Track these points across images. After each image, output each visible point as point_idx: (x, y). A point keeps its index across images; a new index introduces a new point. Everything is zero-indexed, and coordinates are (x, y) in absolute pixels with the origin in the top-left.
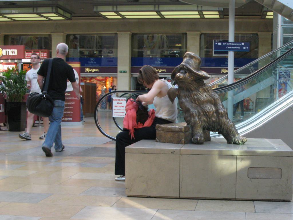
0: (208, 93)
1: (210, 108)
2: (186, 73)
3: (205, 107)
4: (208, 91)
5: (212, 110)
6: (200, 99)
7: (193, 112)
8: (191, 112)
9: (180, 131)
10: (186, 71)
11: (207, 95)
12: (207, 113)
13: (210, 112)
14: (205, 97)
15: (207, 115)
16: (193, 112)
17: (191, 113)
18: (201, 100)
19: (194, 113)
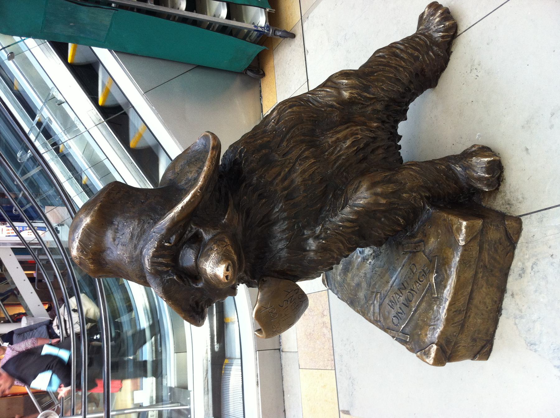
2: (196, 240)
6: (306, 175)
7: (376, 194)
12: (362, 145)
16: (376, 194)
17: (383, 201)
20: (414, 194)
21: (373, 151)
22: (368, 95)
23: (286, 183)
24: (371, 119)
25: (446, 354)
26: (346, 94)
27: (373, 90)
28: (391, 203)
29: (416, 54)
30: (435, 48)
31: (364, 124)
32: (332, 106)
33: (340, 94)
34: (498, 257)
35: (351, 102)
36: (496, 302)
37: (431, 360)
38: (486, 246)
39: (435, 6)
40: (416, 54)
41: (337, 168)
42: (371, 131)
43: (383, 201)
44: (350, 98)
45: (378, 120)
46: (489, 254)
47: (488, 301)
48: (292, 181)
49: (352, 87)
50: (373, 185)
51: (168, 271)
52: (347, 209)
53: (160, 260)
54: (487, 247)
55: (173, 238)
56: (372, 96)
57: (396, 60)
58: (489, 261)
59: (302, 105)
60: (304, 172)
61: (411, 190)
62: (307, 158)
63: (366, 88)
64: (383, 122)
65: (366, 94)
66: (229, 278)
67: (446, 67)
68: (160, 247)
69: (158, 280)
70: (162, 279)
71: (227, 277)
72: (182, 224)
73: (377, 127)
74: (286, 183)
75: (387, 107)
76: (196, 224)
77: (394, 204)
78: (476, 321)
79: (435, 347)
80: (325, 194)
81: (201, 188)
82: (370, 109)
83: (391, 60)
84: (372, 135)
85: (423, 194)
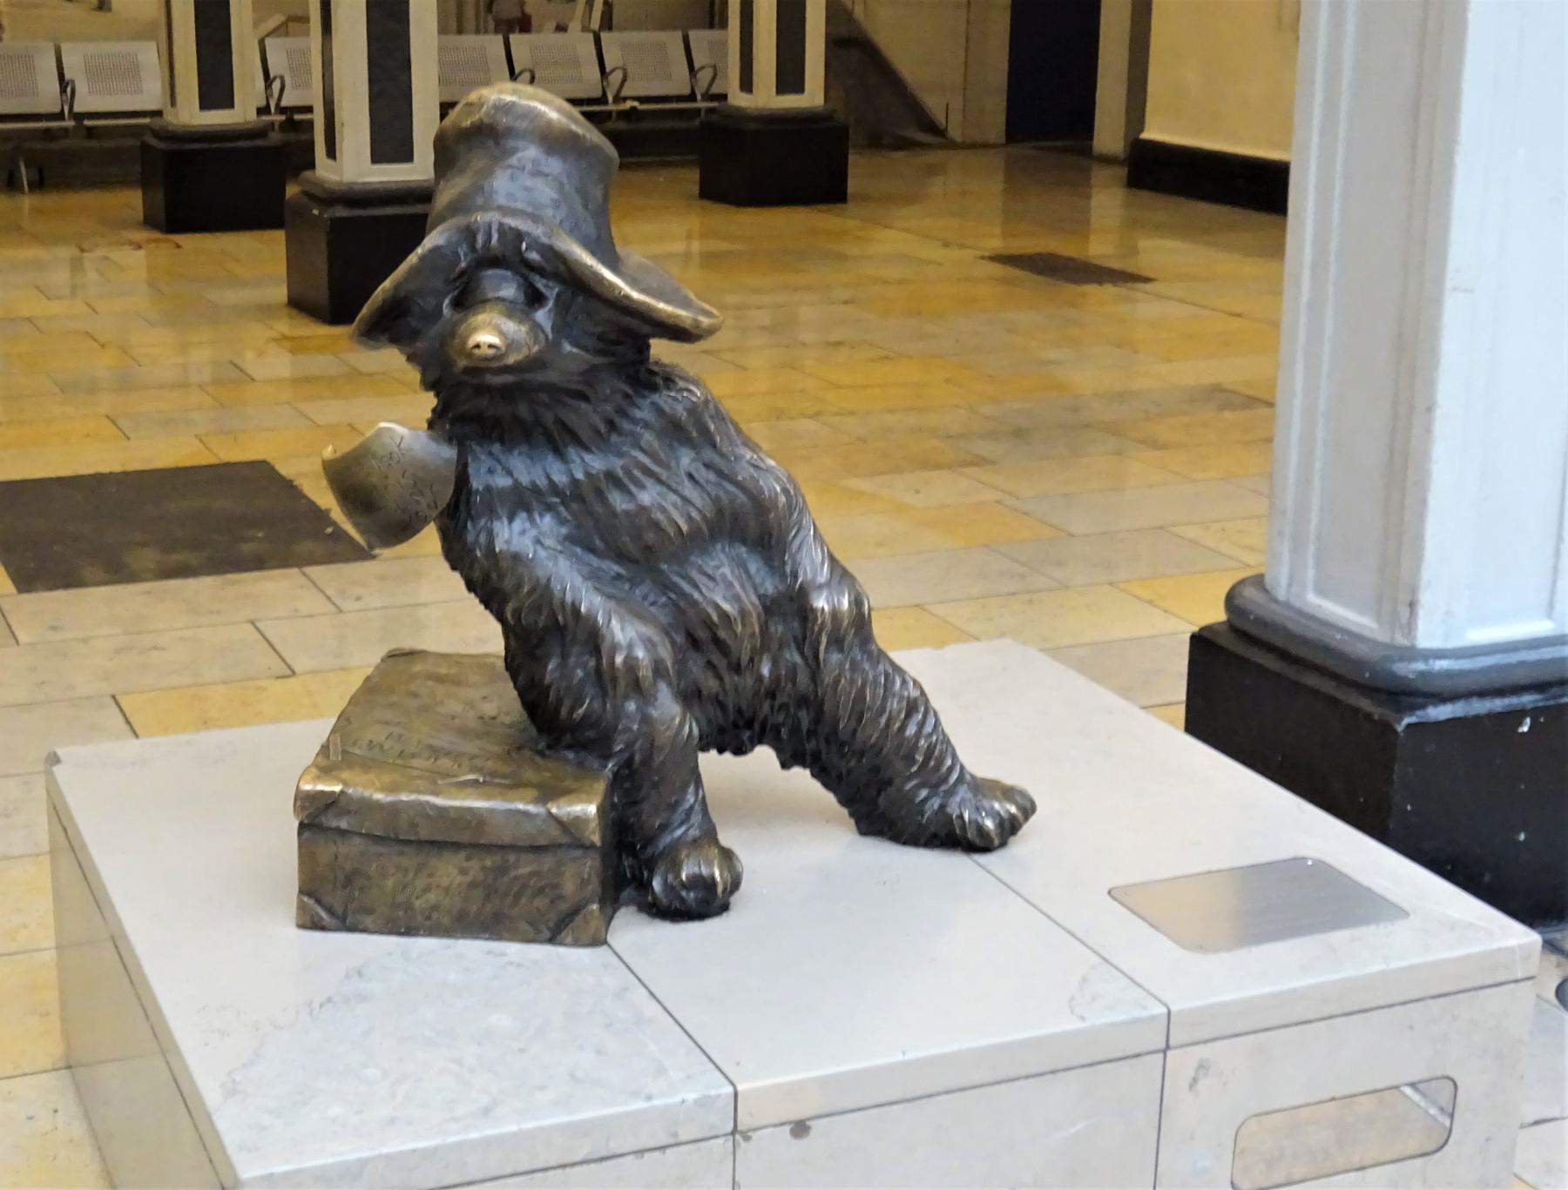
0: (708, 454)
1: (726, 586)
2: (535, 298)
3: (695, 574)
4: (704, 431)
5: (757, 602)
6: (660, 516)
7: (630, 646)
8: (614, 648)
9: (565, 840)
10: (540, 284)
11: (703, 475)
12: (722, 634)
13: (743, 613)
14: (689, 490)
15: (717, 641)
16: (630, 646)
17: (619, 660)
18: (672, 531)
19: (640, 653)
20: (635, 727)
21: (710, 665)
22: (822, 648)
23: (637, 473)
24: (775, 663)
25: (316, 818)
26: (821, 603)
27: (835, 657)
28: (614, 680)
29: (920, 758)
30: (935, 803)
31: (765, 647)
32: (795, 575)
33: (820, 587)
34: (524, 900)
35: (805, 613)
36: (429, 918)
37: (307, 787)
38: (548, 862)
39: (1028, 810)
40: (920, 758)
41: (675, 584)
42: (751, 660)
43: (619, 660)
44: (813, 610)
45: (776, 679)
46: (533, 874)
47: (432, 897)
48: (642, 487)
49: (835, 614)
50: (649, 644)
51: (473, 248)
52: (598, 600)
53: (495, 237)
54: (546, 867)
55: (534, 256)
56: (821, 656)
57: (899, 712)
58: (516, 878)
59: (791, 515)
60: (664, 510)
61: (646, 720)
62: (690, 519)
63: (837, 642)
64: (772, 695)
65: (824, 640)
66: (476, 351)
67: (905, 843)
68: (519, 236)
69: (454, 239)
70: (458, 244)
71: (478, 346)
72: (562, 268)
73: (760, 678)
74: (637, 473)
75: (803, 701)
76: (558, 296)
77: (615, 687)
78: (391, 874)
79: (337, 788)
80: (620, 556)
81: (627, 297)
82: (798, 659)
83: (899, 702)
84: (744, 662)
85: (637, 746)
